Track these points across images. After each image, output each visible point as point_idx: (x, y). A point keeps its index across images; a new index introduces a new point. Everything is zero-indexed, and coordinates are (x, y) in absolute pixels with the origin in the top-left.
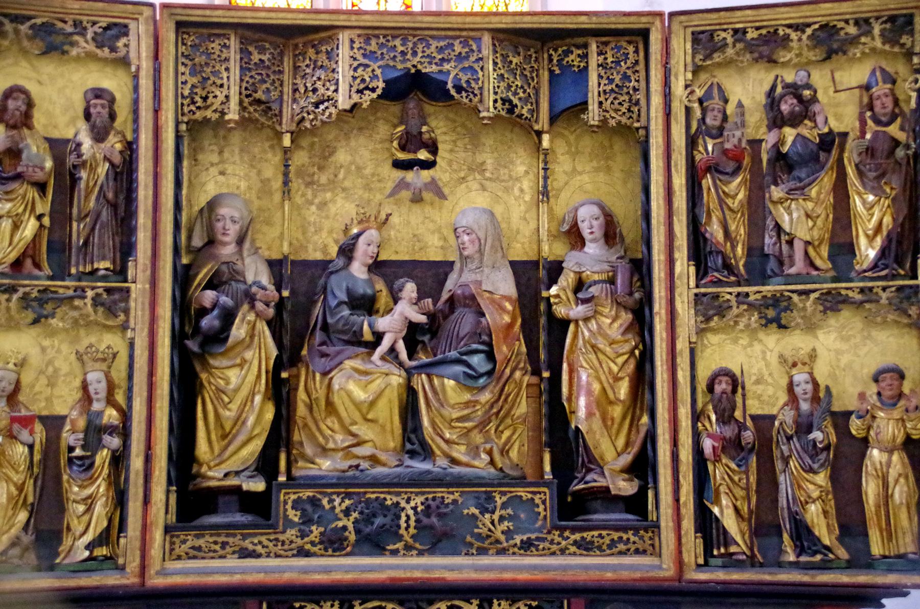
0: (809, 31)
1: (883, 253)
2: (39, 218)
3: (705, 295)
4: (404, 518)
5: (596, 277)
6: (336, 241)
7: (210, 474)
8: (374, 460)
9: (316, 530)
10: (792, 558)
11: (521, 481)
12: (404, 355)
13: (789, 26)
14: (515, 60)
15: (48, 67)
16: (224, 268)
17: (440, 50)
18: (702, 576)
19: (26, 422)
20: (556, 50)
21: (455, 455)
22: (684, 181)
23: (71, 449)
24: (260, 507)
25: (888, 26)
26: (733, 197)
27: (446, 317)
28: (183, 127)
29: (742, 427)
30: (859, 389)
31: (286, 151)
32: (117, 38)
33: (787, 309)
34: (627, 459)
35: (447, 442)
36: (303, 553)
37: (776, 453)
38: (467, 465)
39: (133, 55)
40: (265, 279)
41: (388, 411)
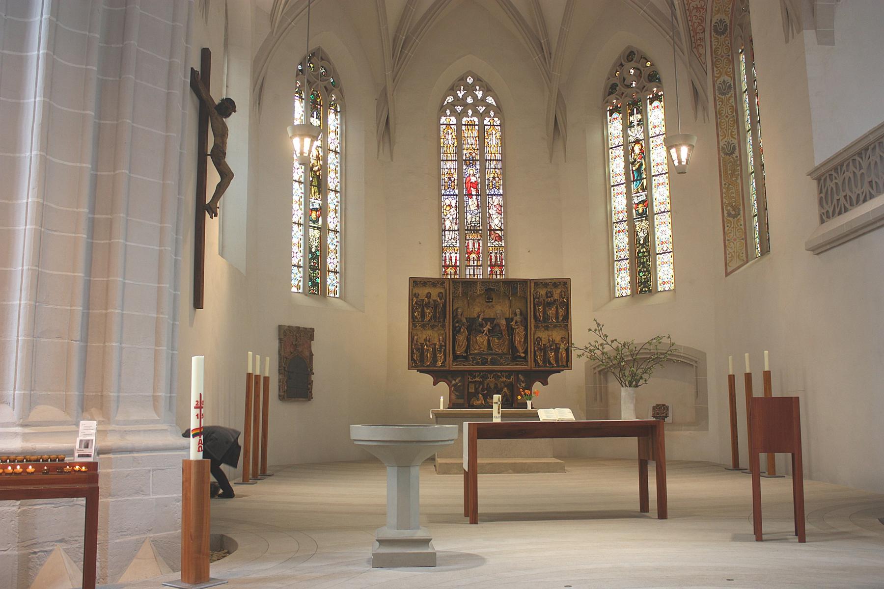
24: (466, 358)
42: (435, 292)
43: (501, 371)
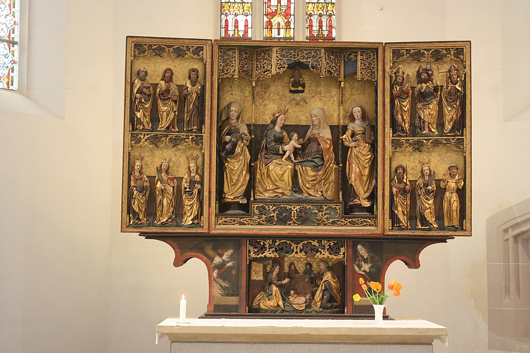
0: (431, 51)
1: (453, 127)
2: (175, 112)
3: (395, 140)
4: (293, 213)
5: (359, 132)
6: (270, 118)
7: (229, 197)
8: (283, 194)
9: (264, 217)
10: (420, 227)
11: (331, 201)
12: (293, 158)
13: (424, 49)
14: (332, 57)
15: (177, 62)
16: (232, 128)
17: (307, 54)
18: (391, 233)
19: (172, 179)
20: (346, 53)
21: (310, 193)
22: (389, 101)
23: (186, 188)
25: (456, 51)
26: (405, 107)
27: (307, 145)
28: (220, 80)
29: (406, 184)
30: (444, 172)
31: (253, 87)
32: (200, 52)
33: (422, 145)
34: (368, 194)
35: (307, 188)
36: (259, 224)
37: (417, 193)
38: (314, 196)
39: (204, 57)
40: (246, 132)
41: (287, 177)
42: (181, 70)
43: (319, 238)
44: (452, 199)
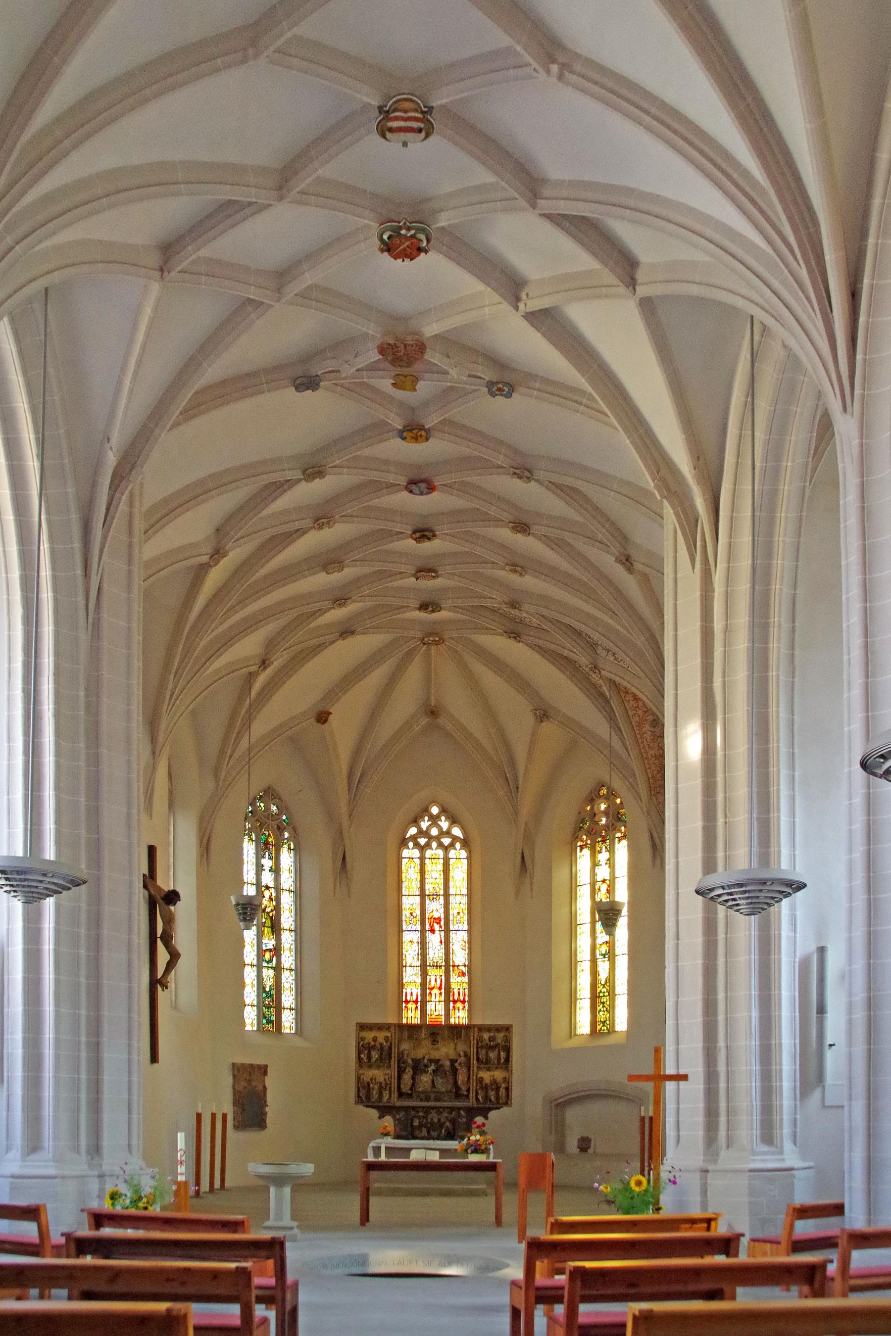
41: (430, 1082)
43: (444, 1108)
44: (502, 1092)
